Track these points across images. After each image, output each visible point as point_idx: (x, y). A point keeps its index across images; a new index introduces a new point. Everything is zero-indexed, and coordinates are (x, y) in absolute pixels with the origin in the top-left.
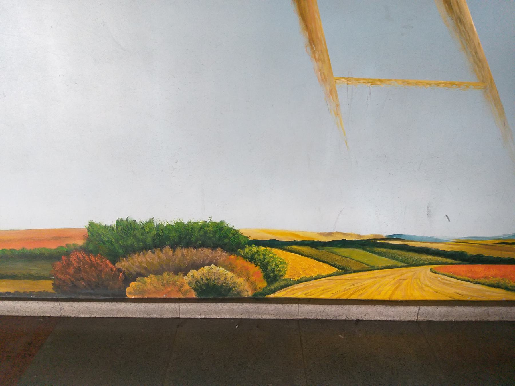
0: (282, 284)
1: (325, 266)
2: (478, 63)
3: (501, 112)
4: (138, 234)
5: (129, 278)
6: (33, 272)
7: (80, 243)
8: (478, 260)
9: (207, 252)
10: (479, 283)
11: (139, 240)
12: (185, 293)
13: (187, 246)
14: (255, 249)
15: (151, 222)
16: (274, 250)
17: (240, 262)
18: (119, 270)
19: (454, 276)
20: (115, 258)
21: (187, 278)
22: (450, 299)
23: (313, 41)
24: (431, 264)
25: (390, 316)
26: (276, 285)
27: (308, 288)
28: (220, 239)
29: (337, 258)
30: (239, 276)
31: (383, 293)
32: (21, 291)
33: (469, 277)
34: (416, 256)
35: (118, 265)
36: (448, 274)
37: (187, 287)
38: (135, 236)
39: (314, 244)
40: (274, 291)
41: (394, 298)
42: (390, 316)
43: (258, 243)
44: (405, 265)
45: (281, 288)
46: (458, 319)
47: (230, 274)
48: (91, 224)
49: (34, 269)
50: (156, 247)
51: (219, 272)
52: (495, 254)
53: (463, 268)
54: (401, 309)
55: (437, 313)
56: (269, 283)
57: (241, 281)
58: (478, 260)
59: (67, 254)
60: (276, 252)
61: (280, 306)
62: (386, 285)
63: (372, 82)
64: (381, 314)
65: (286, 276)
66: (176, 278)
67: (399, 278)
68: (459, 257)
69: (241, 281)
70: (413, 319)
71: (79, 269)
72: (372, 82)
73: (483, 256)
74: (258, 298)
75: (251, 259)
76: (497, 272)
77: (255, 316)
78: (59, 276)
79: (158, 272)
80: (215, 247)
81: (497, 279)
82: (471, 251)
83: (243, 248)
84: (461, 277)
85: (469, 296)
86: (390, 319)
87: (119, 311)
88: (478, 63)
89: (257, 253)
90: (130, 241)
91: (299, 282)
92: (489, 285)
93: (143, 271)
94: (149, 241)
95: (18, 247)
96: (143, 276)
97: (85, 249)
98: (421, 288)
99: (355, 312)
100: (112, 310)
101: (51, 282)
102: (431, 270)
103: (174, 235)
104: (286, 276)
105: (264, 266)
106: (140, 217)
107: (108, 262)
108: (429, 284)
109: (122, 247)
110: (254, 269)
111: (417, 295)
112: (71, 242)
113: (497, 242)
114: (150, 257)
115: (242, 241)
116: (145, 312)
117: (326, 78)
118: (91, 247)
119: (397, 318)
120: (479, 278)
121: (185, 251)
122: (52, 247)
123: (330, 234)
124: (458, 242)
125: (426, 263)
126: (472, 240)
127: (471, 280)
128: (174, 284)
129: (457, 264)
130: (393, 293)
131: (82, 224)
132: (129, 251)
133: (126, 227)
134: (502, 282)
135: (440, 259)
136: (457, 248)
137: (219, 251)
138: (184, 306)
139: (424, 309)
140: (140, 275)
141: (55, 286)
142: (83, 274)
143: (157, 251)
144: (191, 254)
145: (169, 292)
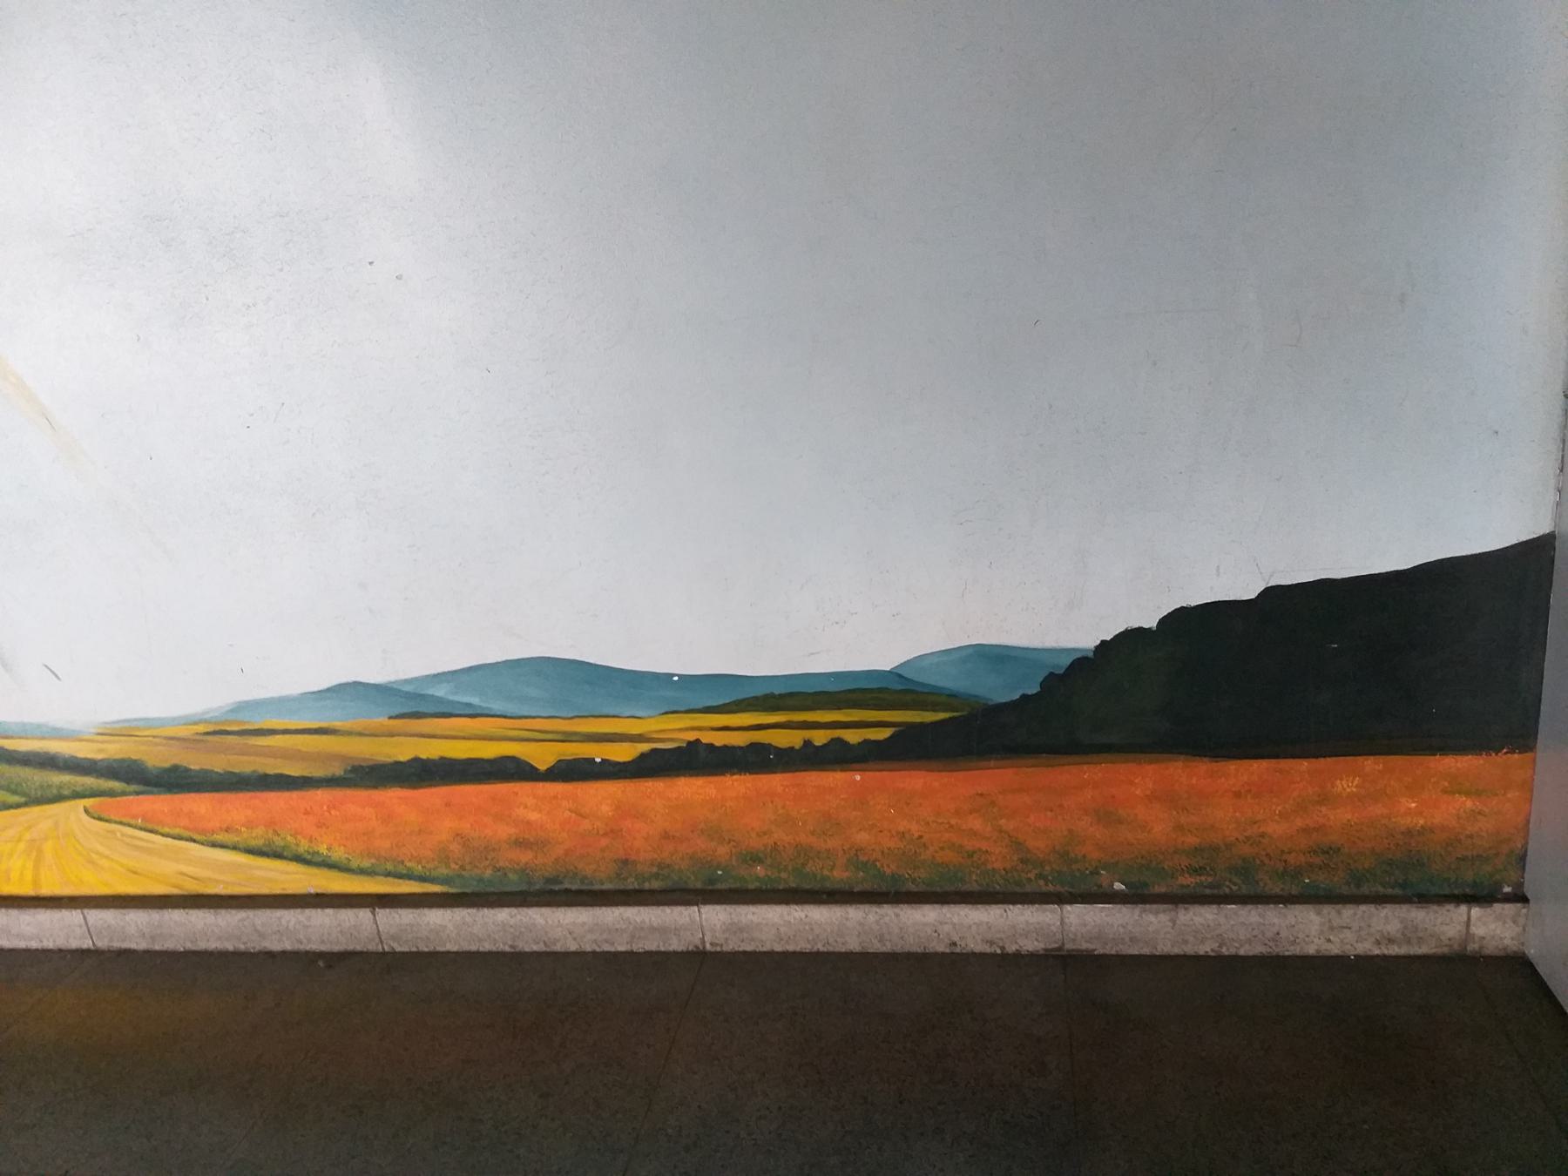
8: (175, 781)
10: (223, 846)
19: (150, 826)
22: (175, 891)
24: (77, 795)
25: (31, 939)
31: (14, 875)
33: (187, 829)
36: (133, 822)
41: (46, 891)
42: (31, 939)
44: (23, 800)
46: (189, 946)
52: (218, 764)
53: (160, 803)
54: (45, 917)
58: (175, 781)
62: (10, 855)
67: (27, 836)
68: (133, 776)
70: (85, 946)
73: (187, 770)
76: (249, 812)
81: (260, 831)
82: (157, 758)
84: (166, 830)
85: (217, 881)
86: (34, 945)
92: (250, 851)
98: (91, 862)
102: (86, 811)
108: (107, 852)
113: (201, 728)
119: (49, 944)
120: (213, 832)
125: (66, 792)
126: (138, 728)
127: (196, 837)
129: (138, 793)
130: (36, 882)
134: (278, 842)
135: (90, 781)
139: (97, 917)
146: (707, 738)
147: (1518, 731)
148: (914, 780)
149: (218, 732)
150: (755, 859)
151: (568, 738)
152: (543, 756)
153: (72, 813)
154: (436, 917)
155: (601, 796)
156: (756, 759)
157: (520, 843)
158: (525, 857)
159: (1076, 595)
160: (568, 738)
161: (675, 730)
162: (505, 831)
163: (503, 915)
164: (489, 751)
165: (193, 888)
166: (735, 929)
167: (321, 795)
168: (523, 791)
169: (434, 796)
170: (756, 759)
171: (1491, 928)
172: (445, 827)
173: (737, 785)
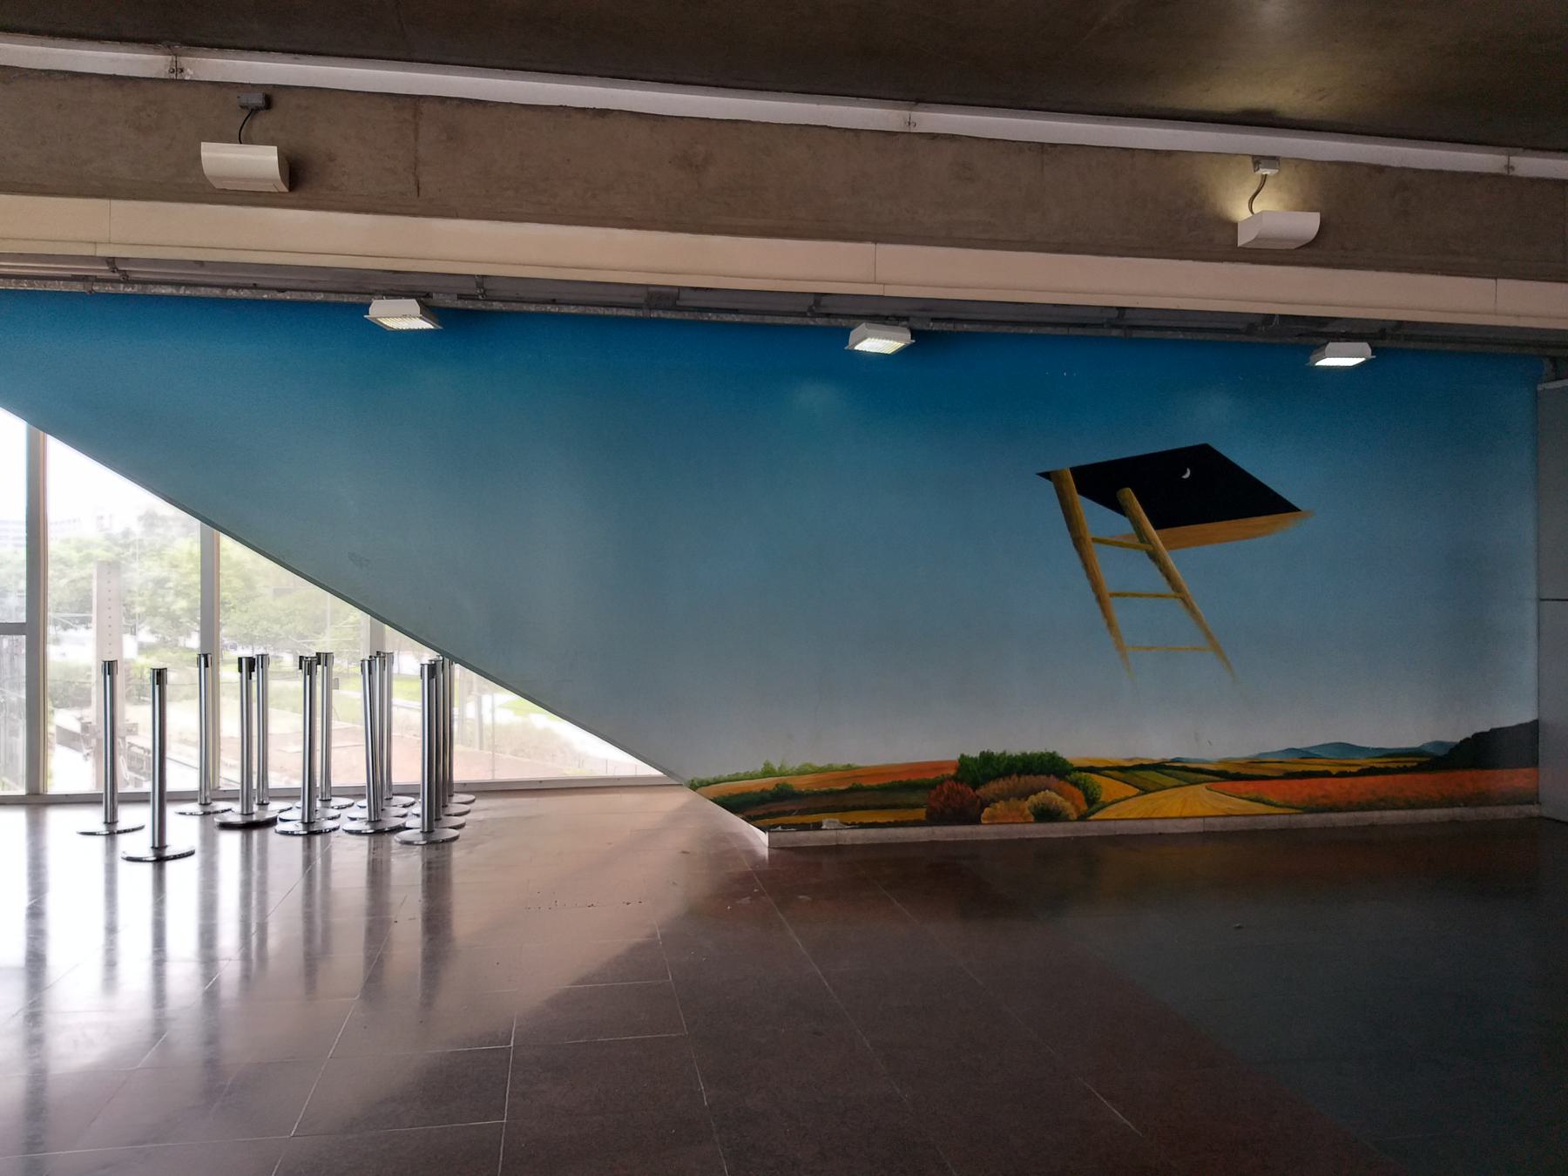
2: (1209, 635)
5: (985, 804)
7: (952, 772)
8: (1237, 777)
9: (1043, 777)
14: (1078, 774)
17: (1068, 787)
21: (1027, 804)
23: (1110, 625)
26: (1095, 807)
28: (1050, 767)
34: (1193, 776)
43: (1081, 769)
49: (914, 798)
51: (1051, 797)
52: (1249, 772)
53: (1229, 785)
54: (1192, 821)
55: (1218, 824)
58: (1237, 777)
59: (941, 783)
60: (1094, 776)
63: (1148, 649)
69: (1067, 804)
72: (1148, 649)
74: (1083, 818)
75: (1075, 784)
79: (1006, 798)
82: (1232, 770)
88: (1209, 635)
95: (904, 778)
97: (955, 778)
99: (1158, 826)
103: (1020, 764)
105: (1085, 790)
106: (997, 750)
110: (1078, 793)
111: (1200, 812)
124: (1220, 762)
131: (955, 757)
132: (988, 778)
133: (987, 758)
136: (1221, 767)
138: (1028, 827)
140: (994, 801)
141: (928, 815)
147: (1534, 762)
148: (1420, 776)
149: (1253, 762)
152: (1334, 770)
153: (1201, 788)
154: (1307, 817)
156: (1385, 771)
159: (1454, 731)
161: (1367, 763)
163: (1324, 816)
164: (1321, 768)
168: (1329, 780)
169: (1304, 782)
170: (1385, 771)
171: (1534, 810)
173: (1380, 778)
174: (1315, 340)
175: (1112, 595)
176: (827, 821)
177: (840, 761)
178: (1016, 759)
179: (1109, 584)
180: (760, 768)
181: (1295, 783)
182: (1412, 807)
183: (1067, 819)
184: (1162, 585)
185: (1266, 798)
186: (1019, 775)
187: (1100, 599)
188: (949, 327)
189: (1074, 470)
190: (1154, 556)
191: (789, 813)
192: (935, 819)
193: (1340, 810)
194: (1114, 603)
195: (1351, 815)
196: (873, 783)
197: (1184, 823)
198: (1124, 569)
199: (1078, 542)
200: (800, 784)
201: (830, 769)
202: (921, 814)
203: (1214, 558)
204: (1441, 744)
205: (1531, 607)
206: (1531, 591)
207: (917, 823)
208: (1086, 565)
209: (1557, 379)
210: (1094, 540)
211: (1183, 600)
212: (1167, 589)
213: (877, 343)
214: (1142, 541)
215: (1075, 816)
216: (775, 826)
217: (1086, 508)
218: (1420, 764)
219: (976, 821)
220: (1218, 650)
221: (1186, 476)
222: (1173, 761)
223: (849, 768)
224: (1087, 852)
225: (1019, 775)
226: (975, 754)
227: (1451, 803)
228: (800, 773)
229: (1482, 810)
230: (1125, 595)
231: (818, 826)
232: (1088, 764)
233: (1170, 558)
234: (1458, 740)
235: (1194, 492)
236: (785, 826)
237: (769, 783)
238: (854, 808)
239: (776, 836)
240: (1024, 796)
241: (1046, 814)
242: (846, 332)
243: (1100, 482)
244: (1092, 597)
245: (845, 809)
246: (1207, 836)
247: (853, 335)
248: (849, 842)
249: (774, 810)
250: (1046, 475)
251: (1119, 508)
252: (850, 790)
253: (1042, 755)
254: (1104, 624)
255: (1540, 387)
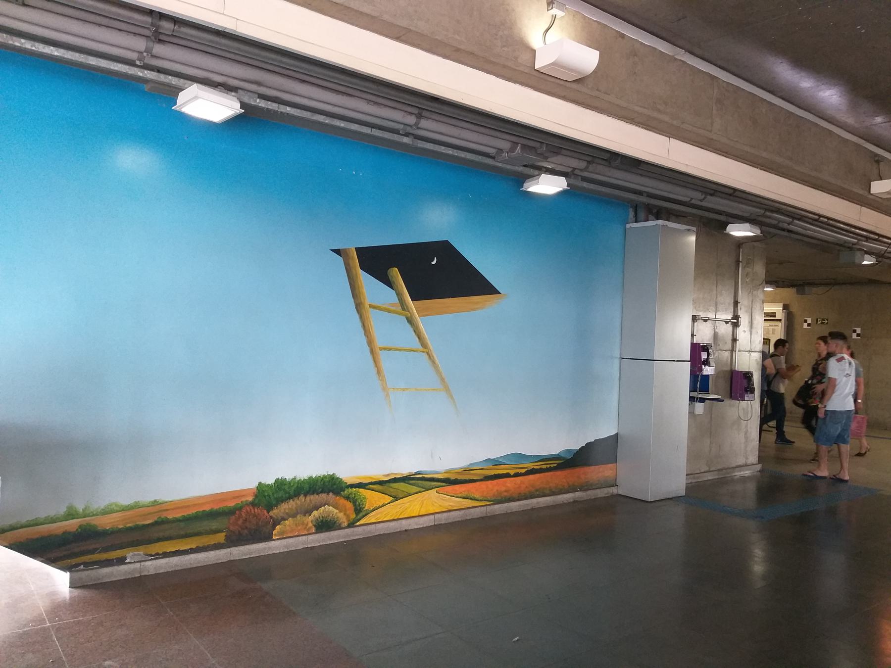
0: (363, 513)
1: (387, 496)
3: (454, 402)
4: (286, 487)
5: (276, 523)
6: (213, 528)
7: (250, 499)
9: (324, 495)
11: (286, 493)
12: (308, 530)
13: (313, 494)
14: (350, 490)
15: (295, 478)
16: (361, 490)
17: (342, 501)
18: (271, 517)
20: (270, 508)
21: (311, 518)
23: (379, 372)
26: (361, 515)
27: (377, 514)
28: (330, 486)
29: (392, 490)
30: (340, 512)
32: (201, 545)
35: (271, 513)
37: (310, 525)
38: (284, 490)
39: (381, 483)
40: (359, 520)
43: (352, 486)
45: (364, 516)
47: (336, 511)
48: (260, 483)
49: (214, 525)
50: (295, 496)
53: (450, 488)
54: (426, 518)
55: (443, 519)
56: (357, 514)
57: (341, 515)
59: (240, 509)
61: (365, 527)
63: (404, 390)
64: (417, 524)
65: (366, 508)
66: (304, 518)
68: (448, 482)
69: (341, 515)
71: (246, 520)
72: (404, 390)
74: (351, 525)
75: (347, 498)
77: (352, 538)
78: (232, 528)
79: (294, 516)
80: (328, 493)
82: (452, 477)
83: (344, 491)
87: (270, 548)
89: (351, 493)
90: (281, 494)
91: (373, 510)
93: (286, 517)
94: (292, 493)
95: (207, 508)
96: (285, 519)
97: (253, 504)
99: (405, 525)
100: (265, 548)
101: (224, 534)
103: (307, 486)
104: (366, 508)
106: (289, 477)
107: (265, 512)
109: (276, 499)
110: (349, 505)
111: (432, 510)
112: (244, 499)
114: (292, 504)
115: (344, 485)
116: (286, 546)
117: (384, 389)
118: (257, 501)
121: (312, 497)
122: (232, 504)
123: (388, 475)
128: (303, 524)
131: (254, 485)
133: (280, 484)
137: (331, 494)
138: (311, 537)
142: (248, 524)
143: (296, 499)
144: (314, 498)
145: (299, 531)
146: (536, 467)
148: (558, 473)
149: (467, 470)
150: (537, 491)
151: (517, 468)
152: (512, 472)
154: (496, 506)
155: (519, 479)
157: (506, 491)
158: (505, 494)
160: (517, 468)
161: (531, 466)
162: (504, 489)
163: (506, 505)
164: (505, 472)
165: (451, 508)
166: (538, 503)
167: (478, 483)
171: (614, 490)
172: (496, 488)
173: (537, 475)
174: (532, 171)
175: (381, 349)
176: (130, 555)
177: (148, 498)
178: (305, 481)
179: (379, 342)
180: (63, 510)
181: (489, 483)
182: (553, 493)
183: (340, 528)
184: (415, 343)
185: (472, 495)
186: (305, 495)
187: (372, 352)
188: (273, 106)
189: (358, 250)
190: (410, 321)
191: (93, 552)
192: (234, 540)
193: (514, 500)
194: (382, 356)
195: (521, 502)
196: (178, 515)
197: (422, 520)
198: (390, 329)
199: (359, 306)
200: (105, 522)
201: (136, 506)
202: (221, 538)
203: (450, 323)
204: (568, 451)
205: (617, 362)
206: (617, 353)
207: (217, 547)
208: (364, 325)
209: (636, 221)
210: (371, 306)
211: (428, 353)
212: (421, 348)
213: (207, 106)
214: (403, 309)
215: (346, 524)
216: (78, 565)
217: (366, 280)
218: (559, 464)
219: (268, 538)
220: (447, 389)
221: (433, 263)
222: (416, 474)
223: (155, 503)
224: (353, 552)
225: (305, 495)
226: (271, 481)
227: (574, 490)
228: (106, 512)
229: (589, 492)
230: (390, 349)
231: (121, 561)
232: (358, 481)
233: (420, 321)
234: (577, 447)
235: (435, 274)
236: (87, 565)
237: (72, 525)
238: (159, 540)
239: (78, 575)
240: (309, 512)
241: (324, 525)
242: (175, 92)
243: (376, 261)
244: (367, 349)
245: (150, 541)
246: (437, 528)
247: (182, 97)
248: (152, 572)
249: (76, 550)
250: (337, 252)
251: (389, 283)
252: (156, 524)
253: (325, 477)
254: (374, 370)
255: (628, 226)
